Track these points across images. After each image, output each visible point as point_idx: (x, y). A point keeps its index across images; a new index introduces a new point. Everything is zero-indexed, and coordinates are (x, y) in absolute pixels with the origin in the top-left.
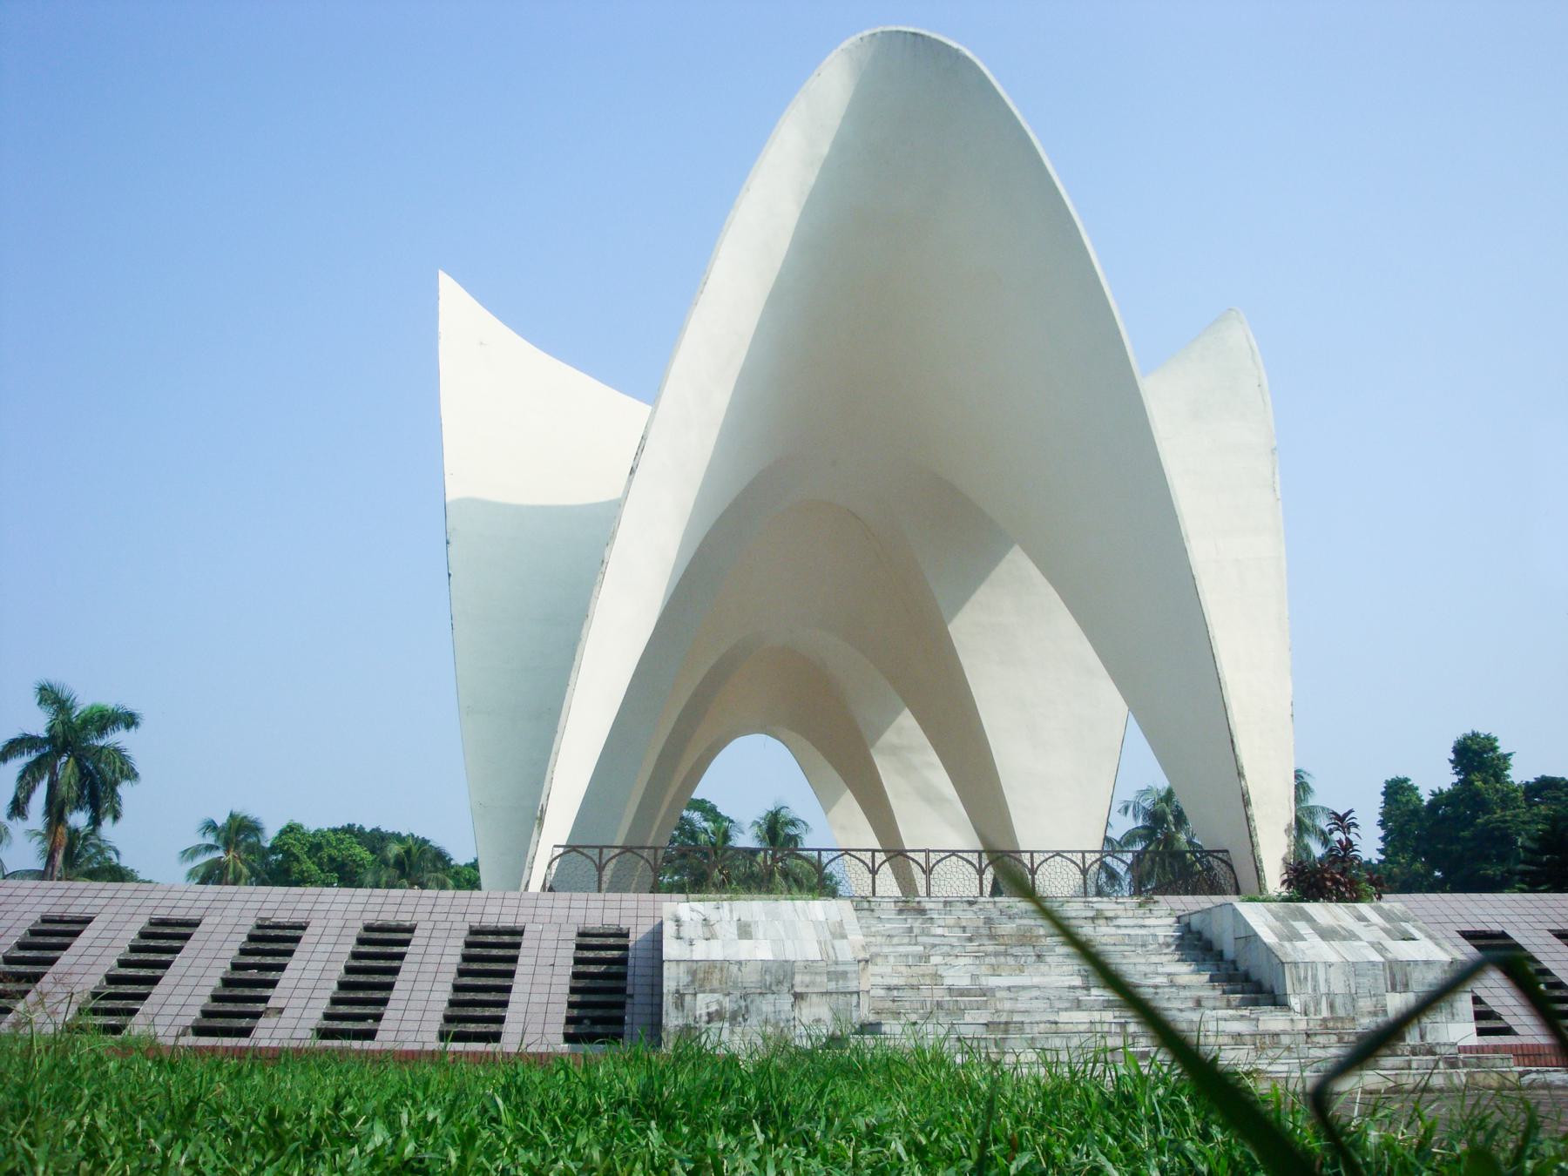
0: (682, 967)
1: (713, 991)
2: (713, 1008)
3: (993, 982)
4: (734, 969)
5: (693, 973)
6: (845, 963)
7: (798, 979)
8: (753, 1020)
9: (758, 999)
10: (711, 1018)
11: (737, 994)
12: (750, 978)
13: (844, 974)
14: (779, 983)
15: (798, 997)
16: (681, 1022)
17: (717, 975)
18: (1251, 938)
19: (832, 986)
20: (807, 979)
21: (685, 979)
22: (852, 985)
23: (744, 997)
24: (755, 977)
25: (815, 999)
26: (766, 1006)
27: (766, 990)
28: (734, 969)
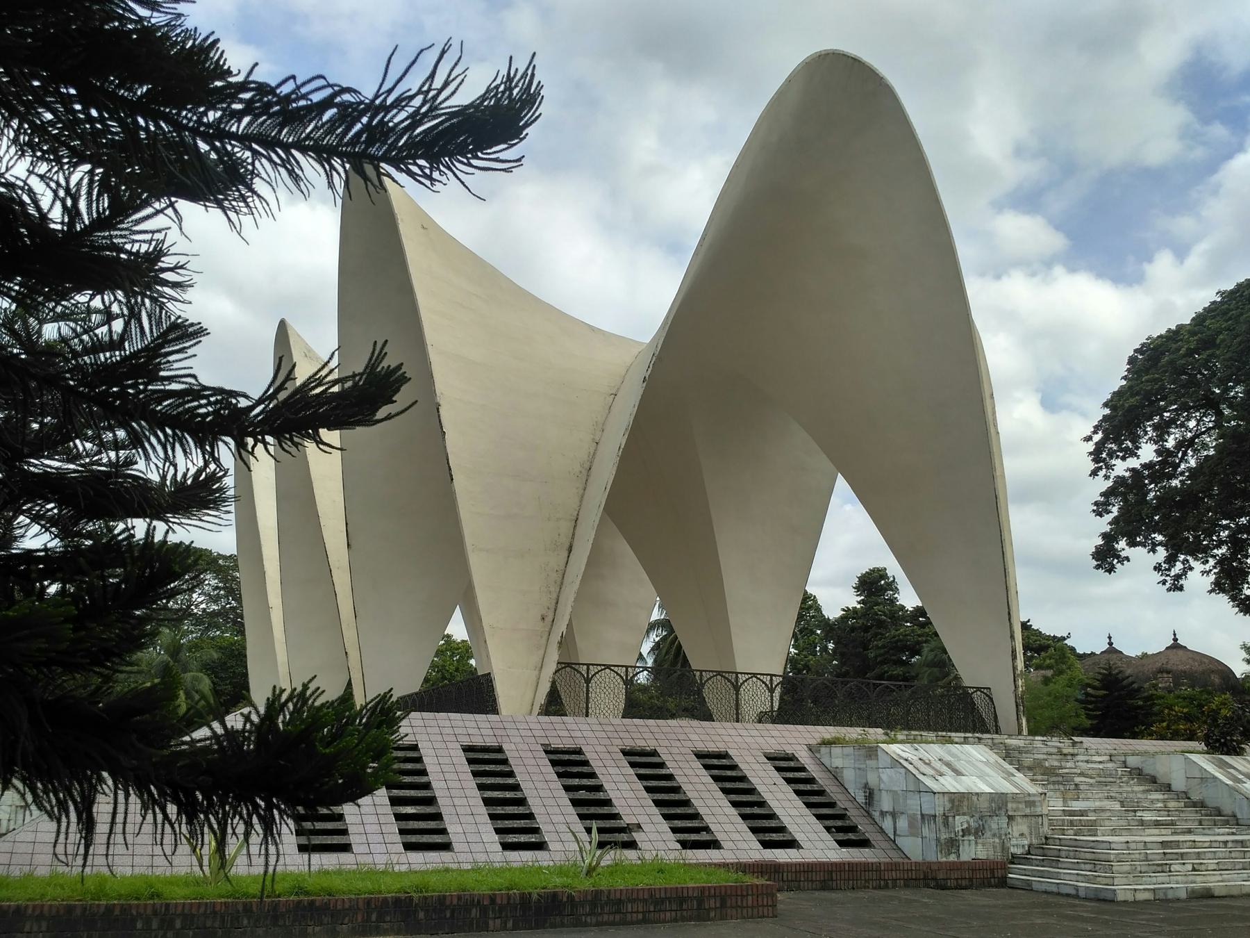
0: (946, 798)
1: (964, 814)
2: (965, 826)
3: (1077, 806)
4: (975, 798)
5: (952, 801)
6: (1034, 795)
7: (1010, 805)
8: (988, 834)
9: (989, 820)
10: (966, 832)
11: (977, 816)
12: (984, 805)
13: (1031, 804)
14: (1000, 809)
15: (1011, 818)
16: (947, 836)
17: (965, 803)
18: (1206, 779)
19: (1028, 811)
20: (1014, 806)
21: (948, 806)
22: (1038, 810)
23: (981, 818)
24: (986, 805)
25: (1019, 819)
26: (993, 824)
27: (994, 813)
28: (975, 798)
